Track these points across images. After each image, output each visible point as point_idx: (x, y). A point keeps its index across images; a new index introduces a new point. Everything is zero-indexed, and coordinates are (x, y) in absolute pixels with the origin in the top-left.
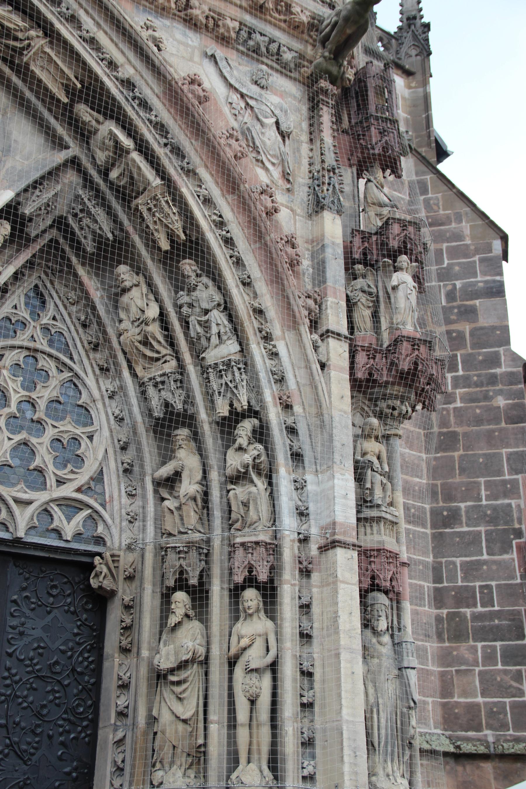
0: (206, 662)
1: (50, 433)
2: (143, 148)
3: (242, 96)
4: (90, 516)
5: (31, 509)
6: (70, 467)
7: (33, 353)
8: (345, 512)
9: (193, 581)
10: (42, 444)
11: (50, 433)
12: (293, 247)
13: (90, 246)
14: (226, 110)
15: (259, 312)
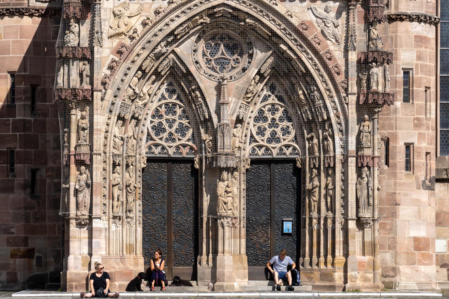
0: (320, 187)
1: (280, 127)
2: (290, 48)
3: (321, 18)
4: (293, 148)
5: (276, 149)
6: (287, 135)
7: (273, 105)
8: (352, 147)
9: (317, 166)
10: (278, 130)
11: (280, 127)
12: (337, 67)
13: (282, 74)
14: (316, 25)
15: (329, 90)
